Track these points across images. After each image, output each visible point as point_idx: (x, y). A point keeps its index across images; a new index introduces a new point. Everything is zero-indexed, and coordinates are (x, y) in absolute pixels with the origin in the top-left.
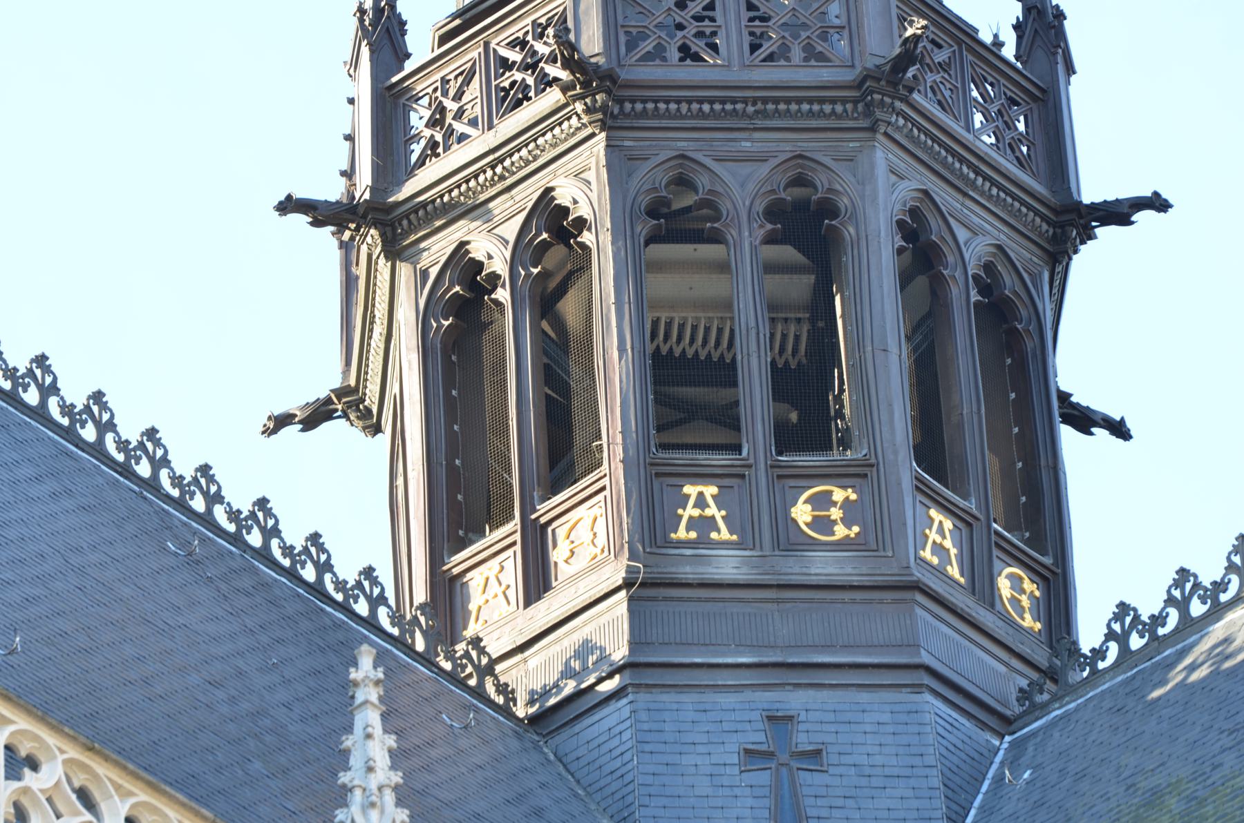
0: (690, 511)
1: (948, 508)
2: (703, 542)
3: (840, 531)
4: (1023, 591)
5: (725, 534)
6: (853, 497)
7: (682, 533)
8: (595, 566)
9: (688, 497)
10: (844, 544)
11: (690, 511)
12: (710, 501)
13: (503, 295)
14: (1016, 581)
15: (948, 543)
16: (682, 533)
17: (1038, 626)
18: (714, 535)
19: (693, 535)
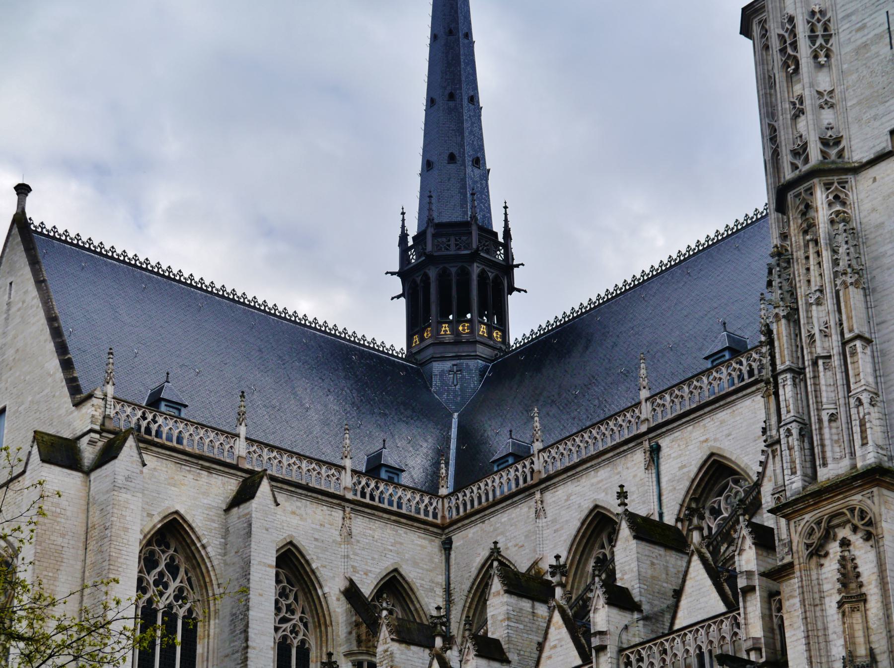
0: (444, 329)
2: (446, 334)
5: (449, 333)
7: (442, 333)
10: (467, 333)
14: (497, 333)
16: (442, 333)
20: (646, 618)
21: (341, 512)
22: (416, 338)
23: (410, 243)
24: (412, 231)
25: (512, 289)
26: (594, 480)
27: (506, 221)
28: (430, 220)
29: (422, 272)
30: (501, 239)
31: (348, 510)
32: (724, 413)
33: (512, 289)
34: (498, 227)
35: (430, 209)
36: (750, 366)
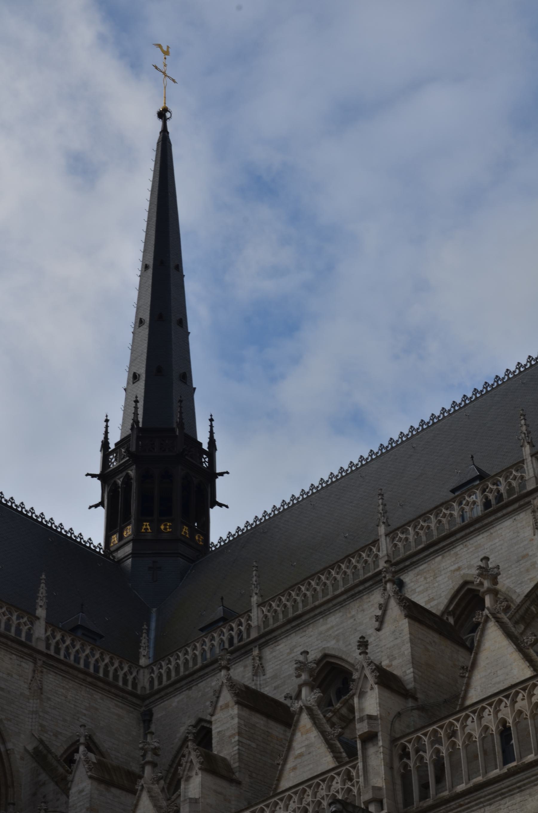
0: (144, 527)
1: (186, 526)
2: (146, 532)
3: (168, 530)
4: (200, 538)
5: (150, 531)
6: (171, 524)
7: (143, 530)
8: (130, 535)
9: (144, 524)
11: (144, 527)
12: (148, 525)
13: (120, 490)
14: (199, 537)
15: (187, 531)
16: (143, 530)
17: (203, 544)
18: (148, 531)
19: (145, 531)
20: (422, 708)
21: (31, 664)
22: (115, 539)
23: (112, 446)
24: (114, 439)
25: (215, 503)
26: (323, 628)
27: (211, 433)
28: (135, 421)
29: (124, 474)
30: (205, 446)
31: (40, 663)
32: (480, 537)
33: (215, 503)
34: (203, 437)
35: (136, 414)
36: (510, 484)
